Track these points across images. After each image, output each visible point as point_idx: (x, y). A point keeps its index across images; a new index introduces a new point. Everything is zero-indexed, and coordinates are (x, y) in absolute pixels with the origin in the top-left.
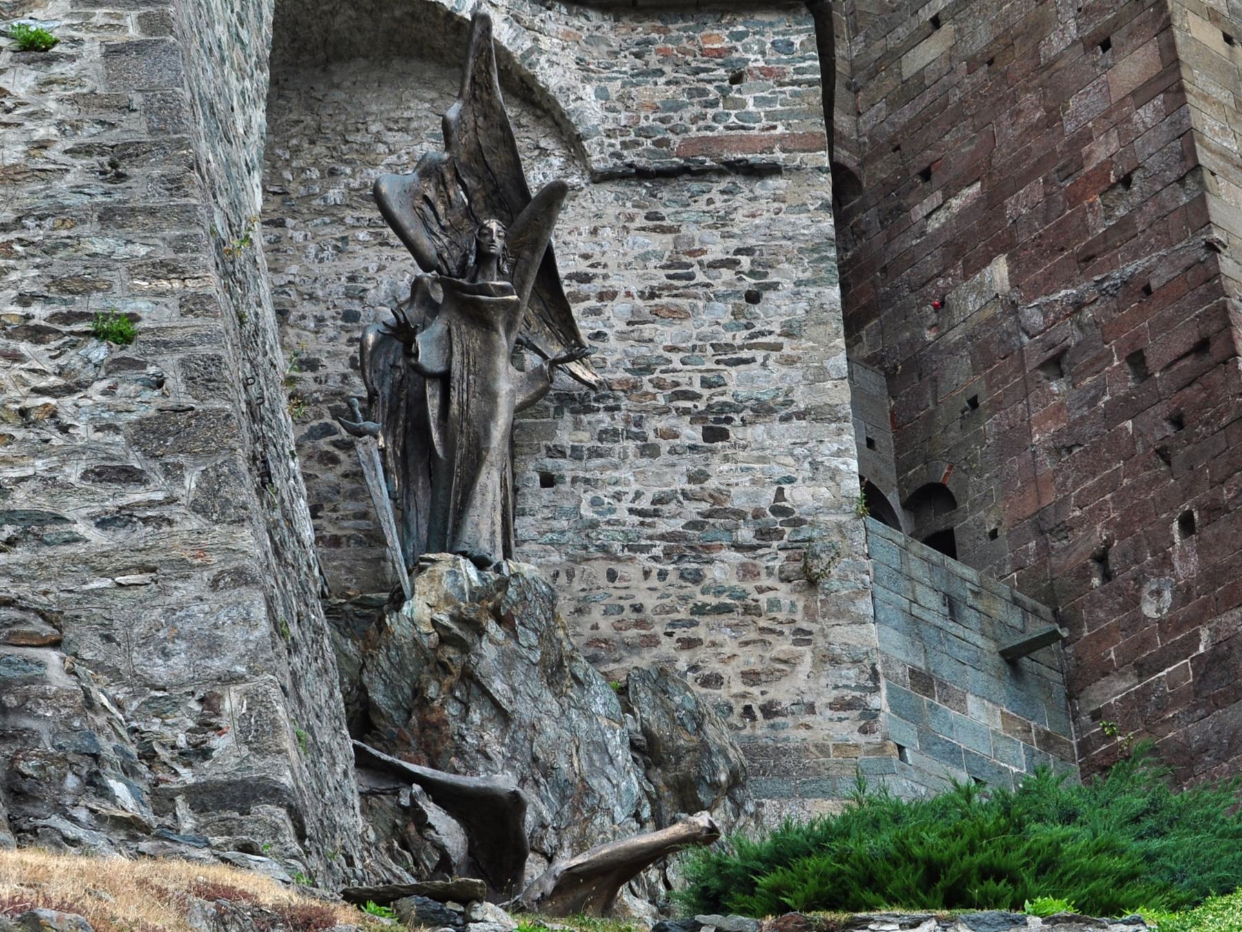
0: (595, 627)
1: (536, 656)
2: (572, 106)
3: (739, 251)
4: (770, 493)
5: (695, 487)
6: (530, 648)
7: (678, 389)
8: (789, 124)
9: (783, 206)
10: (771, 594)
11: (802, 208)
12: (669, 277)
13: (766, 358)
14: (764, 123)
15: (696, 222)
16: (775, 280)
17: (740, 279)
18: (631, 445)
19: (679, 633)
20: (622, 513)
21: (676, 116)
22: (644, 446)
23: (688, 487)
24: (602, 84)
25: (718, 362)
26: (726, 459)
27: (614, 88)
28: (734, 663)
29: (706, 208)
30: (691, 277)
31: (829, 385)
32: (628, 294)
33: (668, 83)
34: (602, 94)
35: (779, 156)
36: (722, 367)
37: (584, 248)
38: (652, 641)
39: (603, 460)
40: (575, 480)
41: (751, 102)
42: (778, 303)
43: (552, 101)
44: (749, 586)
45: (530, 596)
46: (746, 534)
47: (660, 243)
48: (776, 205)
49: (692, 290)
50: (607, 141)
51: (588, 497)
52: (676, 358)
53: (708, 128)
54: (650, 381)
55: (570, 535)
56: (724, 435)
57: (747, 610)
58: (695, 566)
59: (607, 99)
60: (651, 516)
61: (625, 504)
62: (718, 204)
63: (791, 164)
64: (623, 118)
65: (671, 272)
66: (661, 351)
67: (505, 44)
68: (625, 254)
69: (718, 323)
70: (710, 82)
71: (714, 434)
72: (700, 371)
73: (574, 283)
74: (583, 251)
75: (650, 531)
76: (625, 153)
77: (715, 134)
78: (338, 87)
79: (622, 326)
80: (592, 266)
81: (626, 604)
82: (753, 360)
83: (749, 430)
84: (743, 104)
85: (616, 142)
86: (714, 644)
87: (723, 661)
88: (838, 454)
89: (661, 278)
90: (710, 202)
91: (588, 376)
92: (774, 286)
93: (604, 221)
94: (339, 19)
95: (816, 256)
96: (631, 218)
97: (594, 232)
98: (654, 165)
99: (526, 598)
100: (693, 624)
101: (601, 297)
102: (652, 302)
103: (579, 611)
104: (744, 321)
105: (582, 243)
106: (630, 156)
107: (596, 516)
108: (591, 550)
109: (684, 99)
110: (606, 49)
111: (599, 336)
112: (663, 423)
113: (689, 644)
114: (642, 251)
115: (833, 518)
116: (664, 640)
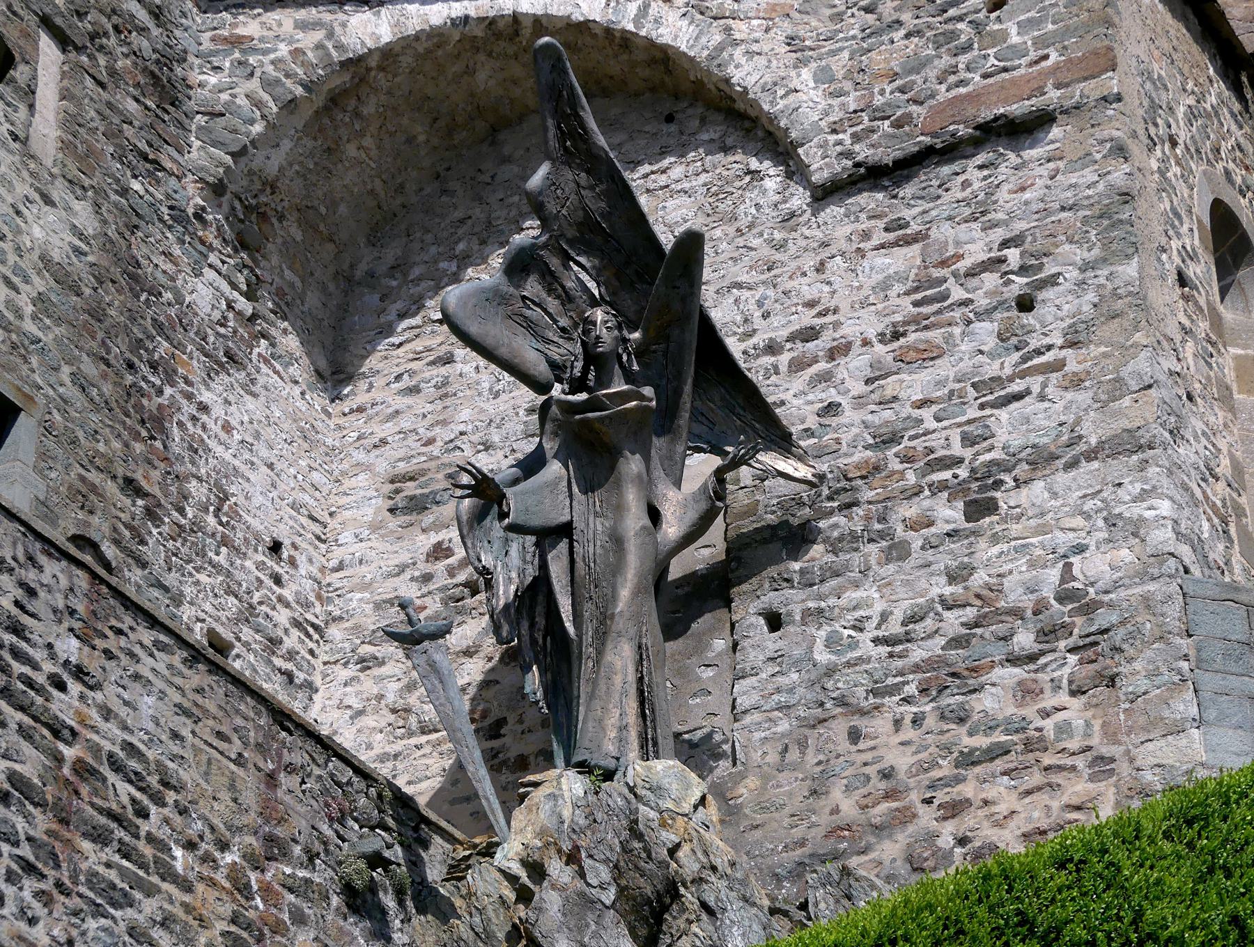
0: (836, 811)
1: (609, 896)
2: (781, 104)
3: (1005, 244)
4: (1053, 575)
5: (957, 589)
6: (602, 887)
7: (932, 456)
8: (1065, 48)
9: (1061, 164)
10: (1060, 716)
11: (1086, 159)
12: (916, 304)
13: (1044, 385)
14: (1033, 55)
15: (950, 218)
16: (1054, 270)
17: (1010, 282)
18: (873, 549)
19: (941, 796)
20: (866, 647)
21: (918, 79)
22: (890, 547)
23: (948, 590)
24: (824, 63)
25: (982, 407)
26: (995, 539)
27: (840, 63)
28: (1012, 824)
29: (960, 196)
30: (944, 297)
31: (1127, 401)
32: (866, 343)
33: (908, 36)
34: (824, 76)
35: (1053, 95)
36: (988, 412)
37: (809, 293)
38: (905, 817)
39: (840, 579)
40: (807, 613)
41: (1014, 30)
42: (1057, 302)
43: (755, 104)
44: (1030, 712)
45: (599, 816)
46: (1024, 640)
47: (904, 260)
48: (1051, 165)
49: (948, 315)
50: (832, 138)
51: (822, 633)
52: (927, 414)
53: (961, 83)
54: (897, 455)
55: (801, 691)
56: (989, 507)
57: (1029, 746)
58: (960, 698)
59: (832, 80)
60: (900, 642)
61: (871, 632)
62: (976, 185)
63: (1068, 103)
64: (852, 102)
65: (918, 296)
66: (907, 410)
67: (683, 48)
68: (860, 288)
69: (981, 352)
70: (960, 19)
71: (979, 509)
72: (959, 425)
73: (799, 345)
74: (808, 297)
75: (899, 663)
76: (857, 148)
77: (970, 88)
78: (507, 160)
79: (858, 388)
80: (820, 315)
81: (871, 770)
82: (1028, 392)
83: (1024, 491)
84: (1005, 35)
85: (846, 137)
86: (986, 802)
87: (998, 825)
88: (1142, 496)
89: (906, 307)
90: (966, 184)
91: (803, 472)
92: (1052, 281)
93: (833, 249)
94: (482, 76)
95: (1106, 222)
96: (866, 235)
97: (820, 268)
98: (887, 155)
99: (595, 821)
100: (959, 780)
101: (832, 355)
102: (896, 345)
103: (814, 792)
104: (1014, 340)
105: (808, 288)
106: (863, 152)
107: (833, 658)
108: (828, 706)
109: (931, 52)
110: (828, 12)
111: (831, 409)
112: (909, 510)
113: (954, 809)
114: (880, 277)
115: (1138, 590)
116: (922, 809)
